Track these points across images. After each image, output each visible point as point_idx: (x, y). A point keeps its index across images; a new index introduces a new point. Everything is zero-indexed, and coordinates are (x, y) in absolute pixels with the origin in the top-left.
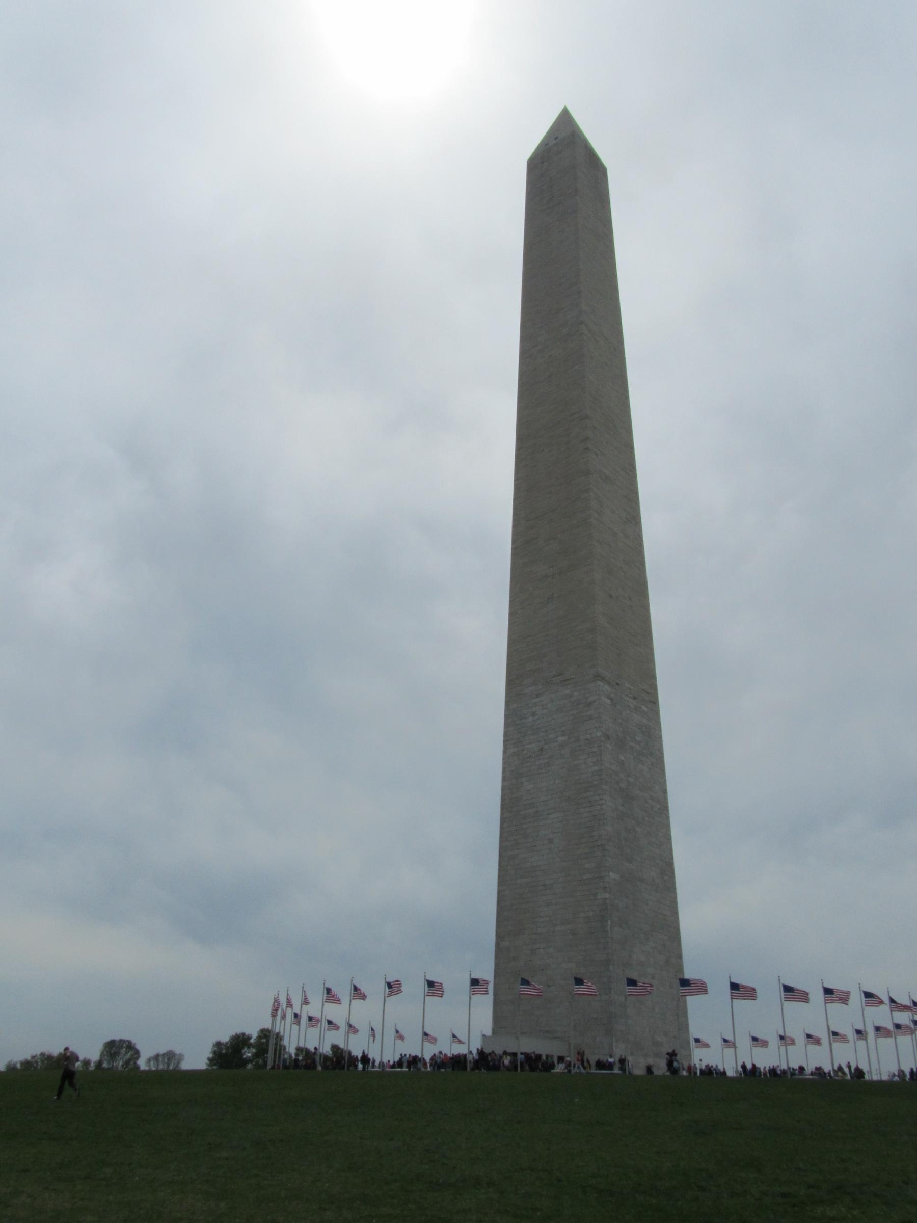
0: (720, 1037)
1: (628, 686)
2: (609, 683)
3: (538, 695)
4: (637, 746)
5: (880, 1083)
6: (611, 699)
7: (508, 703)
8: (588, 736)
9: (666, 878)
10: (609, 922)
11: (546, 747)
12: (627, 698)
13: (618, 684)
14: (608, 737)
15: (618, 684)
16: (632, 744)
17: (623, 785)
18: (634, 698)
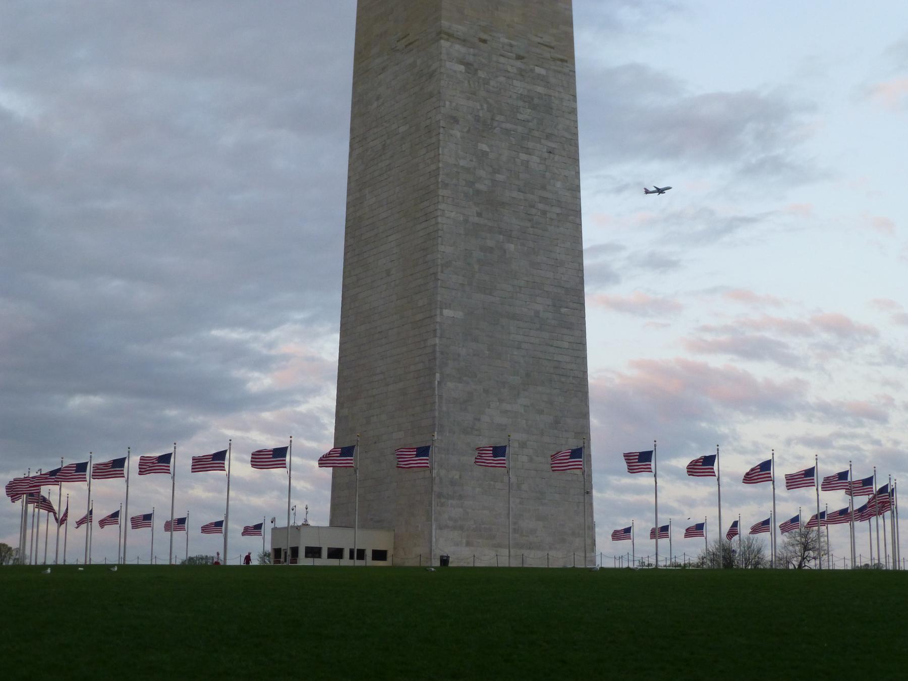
0: (643, 519)
1: (504, 40)
2: (464, 41)
3: (384, 69)
4: (520, 129)
5: (171, 568)
6: (467, 65)
7: (355, 84)
8: (428, 122)
9: (563, 310)
10: (438, 375)
11: (388, 142)
12: (502, 60)
13: (484, 41)
14: (455, 120)
15: (484, 41)
16: (509, 126)
17: (479, 186)
18: (519, 58)
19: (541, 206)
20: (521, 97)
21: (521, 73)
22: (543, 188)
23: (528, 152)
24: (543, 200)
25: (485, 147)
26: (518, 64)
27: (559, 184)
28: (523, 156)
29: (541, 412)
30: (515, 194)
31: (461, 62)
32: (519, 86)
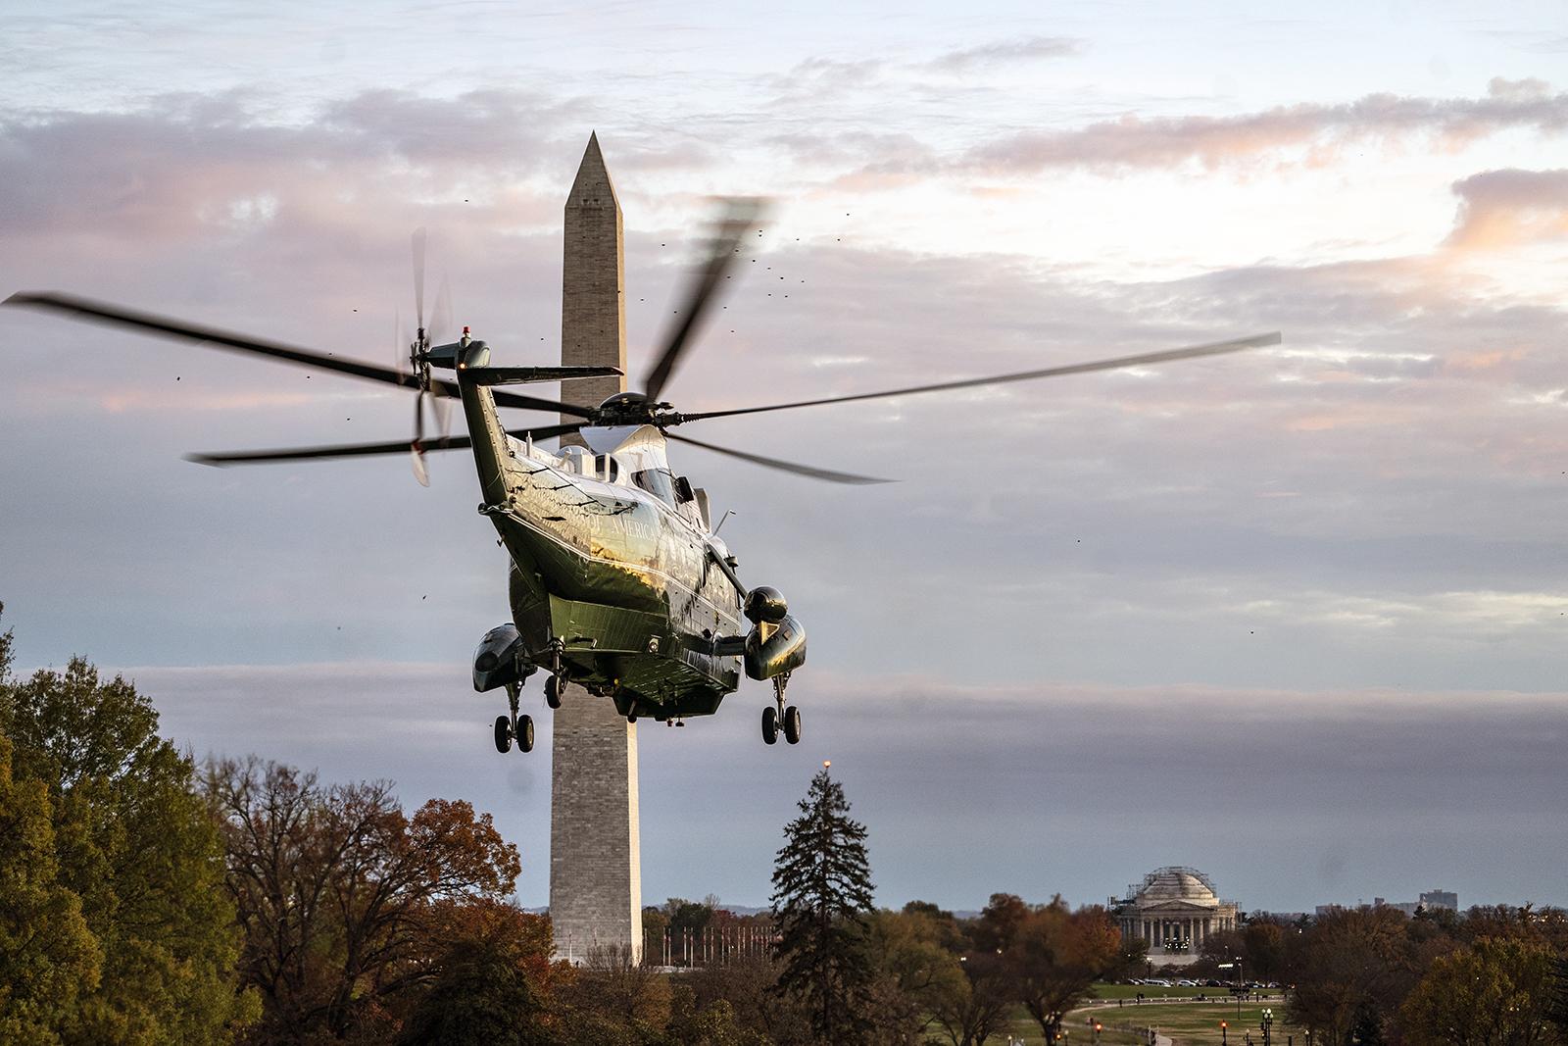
4: (595, 770)
17: (572, 801)
18: (595, 736)
19: (606, 804)
20: (595, 755)
21: (596, 742)
22: (608, 795)
23: (600, 780)
24: (607, 801)
25: (576, 783)
26: (595, 739)
27: (616, 792)
28: (597, 782)
29: (604, 897)
30: (591, 801)
31: (562, 746)
32: (595, 750)
